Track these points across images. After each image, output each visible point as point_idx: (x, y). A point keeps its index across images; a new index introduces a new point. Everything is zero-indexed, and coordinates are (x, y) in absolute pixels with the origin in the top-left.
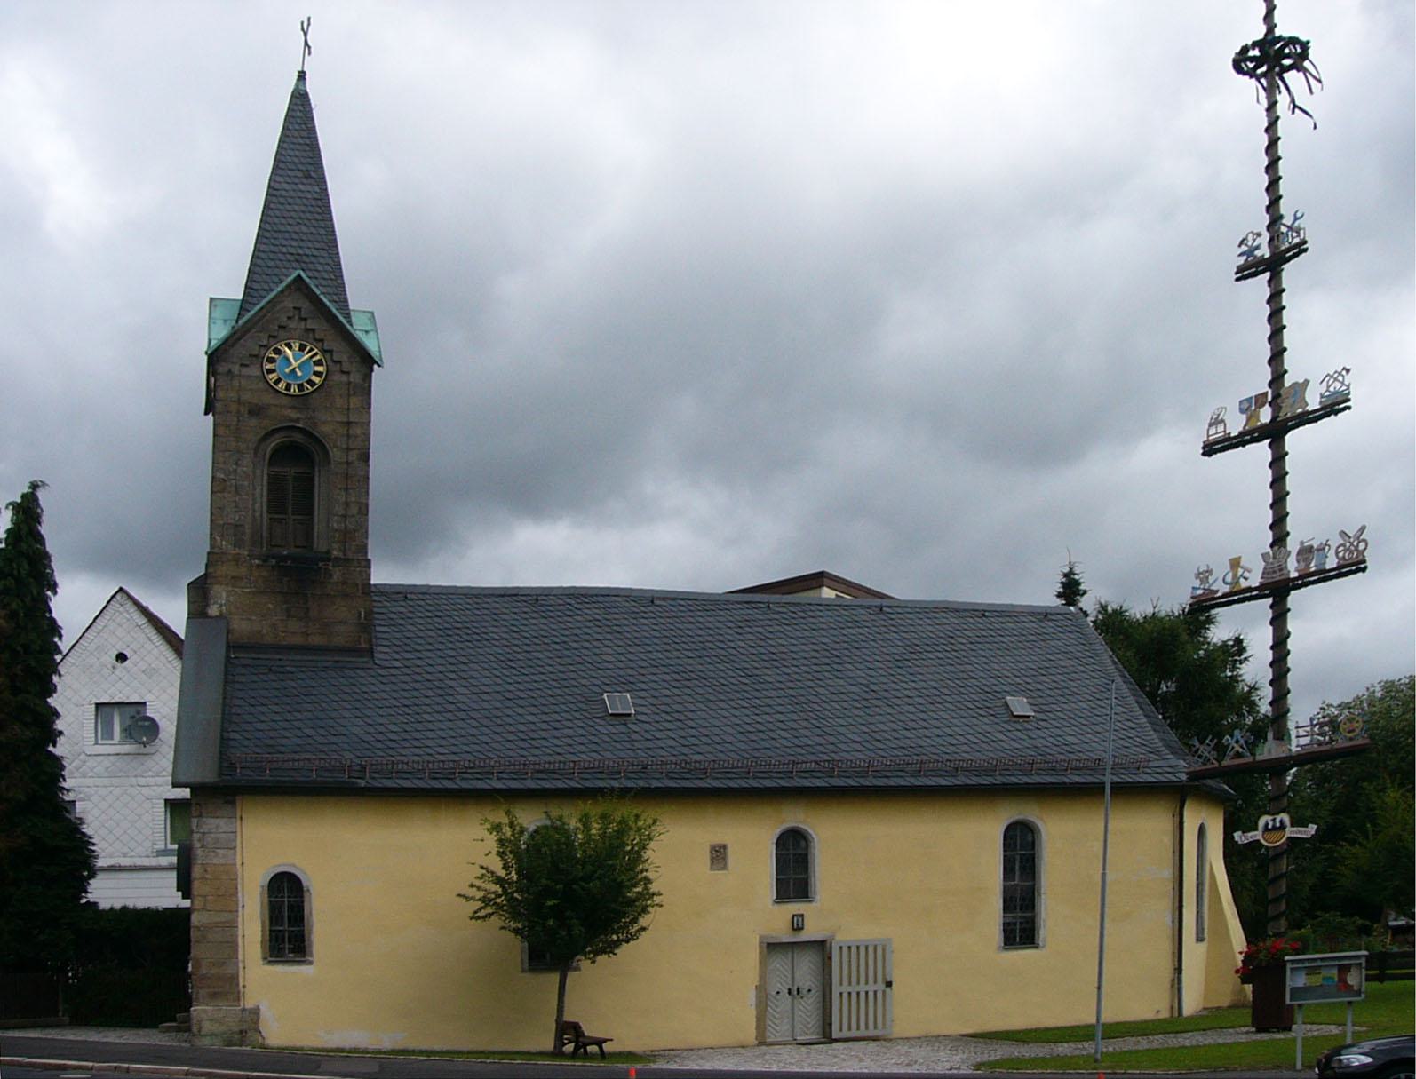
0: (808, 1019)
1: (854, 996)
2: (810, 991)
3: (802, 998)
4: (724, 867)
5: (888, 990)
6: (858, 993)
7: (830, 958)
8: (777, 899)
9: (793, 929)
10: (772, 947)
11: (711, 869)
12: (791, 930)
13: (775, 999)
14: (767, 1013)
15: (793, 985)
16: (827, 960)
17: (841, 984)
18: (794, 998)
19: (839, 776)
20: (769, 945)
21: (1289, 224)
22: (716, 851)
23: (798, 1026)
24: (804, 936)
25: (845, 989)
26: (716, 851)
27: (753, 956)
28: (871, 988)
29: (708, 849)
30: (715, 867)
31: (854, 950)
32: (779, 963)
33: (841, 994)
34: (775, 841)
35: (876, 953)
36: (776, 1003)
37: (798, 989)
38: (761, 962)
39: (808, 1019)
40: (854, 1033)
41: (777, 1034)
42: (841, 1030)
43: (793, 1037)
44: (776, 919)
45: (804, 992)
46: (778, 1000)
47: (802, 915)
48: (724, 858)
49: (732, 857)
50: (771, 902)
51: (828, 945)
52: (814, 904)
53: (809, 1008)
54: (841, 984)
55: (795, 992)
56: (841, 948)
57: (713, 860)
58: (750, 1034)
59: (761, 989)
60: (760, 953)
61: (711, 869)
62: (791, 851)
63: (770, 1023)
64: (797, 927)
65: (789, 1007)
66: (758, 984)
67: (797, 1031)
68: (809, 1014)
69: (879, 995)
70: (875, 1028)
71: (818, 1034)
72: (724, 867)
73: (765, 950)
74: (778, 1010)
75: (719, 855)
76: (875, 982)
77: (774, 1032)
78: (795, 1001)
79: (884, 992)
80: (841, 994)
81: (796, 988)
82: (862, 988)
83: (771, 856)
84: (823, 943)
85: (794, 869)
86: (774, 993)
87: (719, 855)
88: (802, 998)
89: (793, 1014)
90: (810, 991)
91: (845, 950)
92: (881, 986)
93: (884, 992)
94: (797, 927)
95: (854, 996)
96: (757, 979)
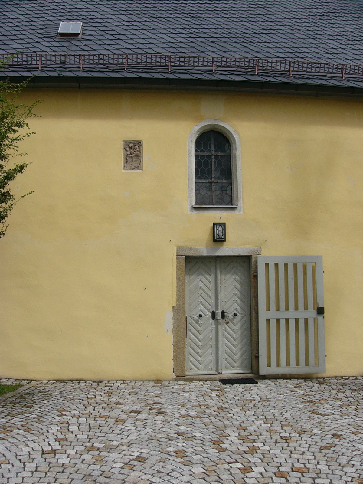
0: (235, 350)
1: (283, 323)
2: (235, 315)
3: (227, 323)
4: (139, 167)
5: (320, 318)
6: (287, 320)
7: (256, 277)
8: (196, 205)
9: (214, 241)
10: (192, 262)
11: (125, 168)
12: (213, 241)
13: (197, 322)
14: (187, 340)
15: (217, 308)
16: (252, 279)
17: (268, 309)
18: (217, 323)
19: (258, 75)
20: (187, 257)
21: (282, 66)
22: (131, 148)
23: (223, 357)
24: (226, 250)
25: (273, 314)
26: (131, 148)
27: (170, 269)
28: (301, 314)
29: (121, 145)
30: (126, 168)
31: (281, 267)
32: (202, 282)
33: (268, 320)
34: (194, 140)
35: (302, 273)
36: (200, 328)
37: (223, 313)
38: (178, 279)
39: (235, 350)
40: (283, 370)
41: (200, 366)
42: (269, 365)
43: (217, 370)
44: (195, 229)
45: (230, 316)
46: (201, 311)
47: (223, 225)
48: (139, 156)
49: (148, 154)
50: (189, 207)
51: (253, 260)
52: (236, 212)
53: (234, 335)
54: (268, 309)
55: (218, 316)
56: (267, 265)
57: (127, 159)
58: (167, 369)
59: (179, 310)
60: (178, 268)
61: (125, 168)
62: (213, 152)
63: (192, 359)
64: (218, 239)
65: (212, 335)
66: (175, 304)
67: (223, 362)
68: (235, 343)
69: (311, 323)
70: (307, 363)
71: (245, 367)
72: (139, 167)
73: (183, 263)
74: (200, 337)
75: (133, 152)
76: (306, 308)
77: (197, 363)
78: (219, 327)
79: (315, 320)
80: (268, 320)
81: (220, 311)
82: (292, 314)
83: (190, 156)
84: (248, 258)
85: (215, 162)
86: (196, 317)
87: (133, 152)
88: (227, 323)
89: (217, 341)
90: (235, 315)
91: (272, 267)
92: (312, 313)
93: (315, 320)
94: (218, 239)
95: (283, 323)
96: (175, 300)
